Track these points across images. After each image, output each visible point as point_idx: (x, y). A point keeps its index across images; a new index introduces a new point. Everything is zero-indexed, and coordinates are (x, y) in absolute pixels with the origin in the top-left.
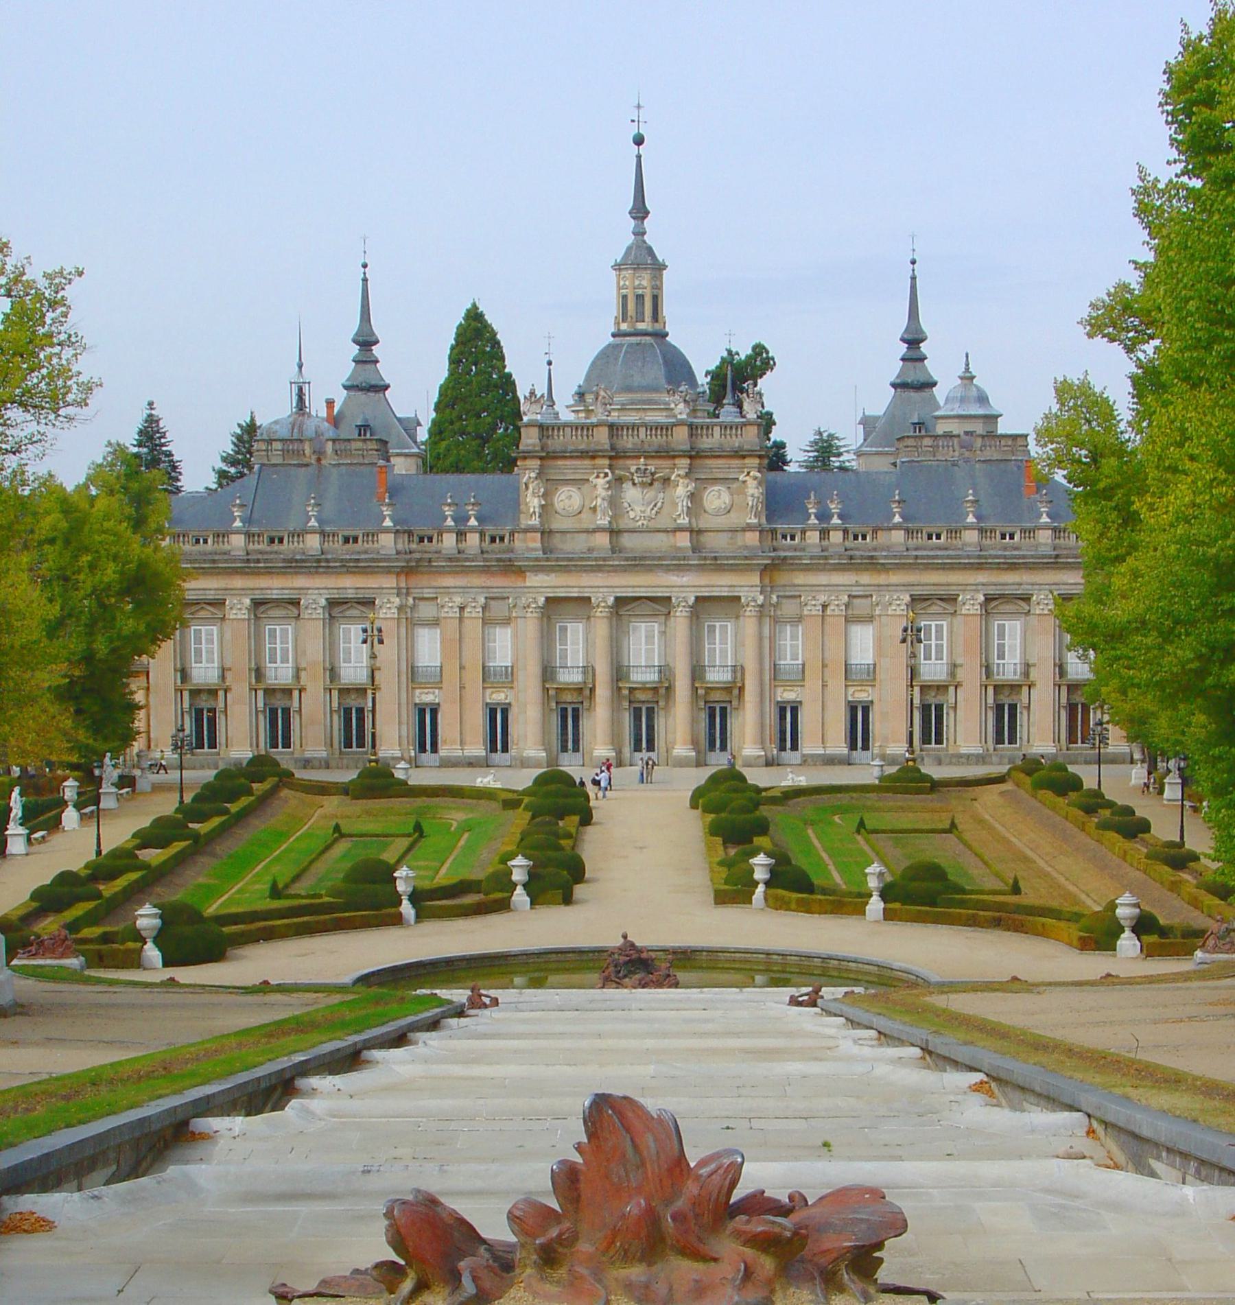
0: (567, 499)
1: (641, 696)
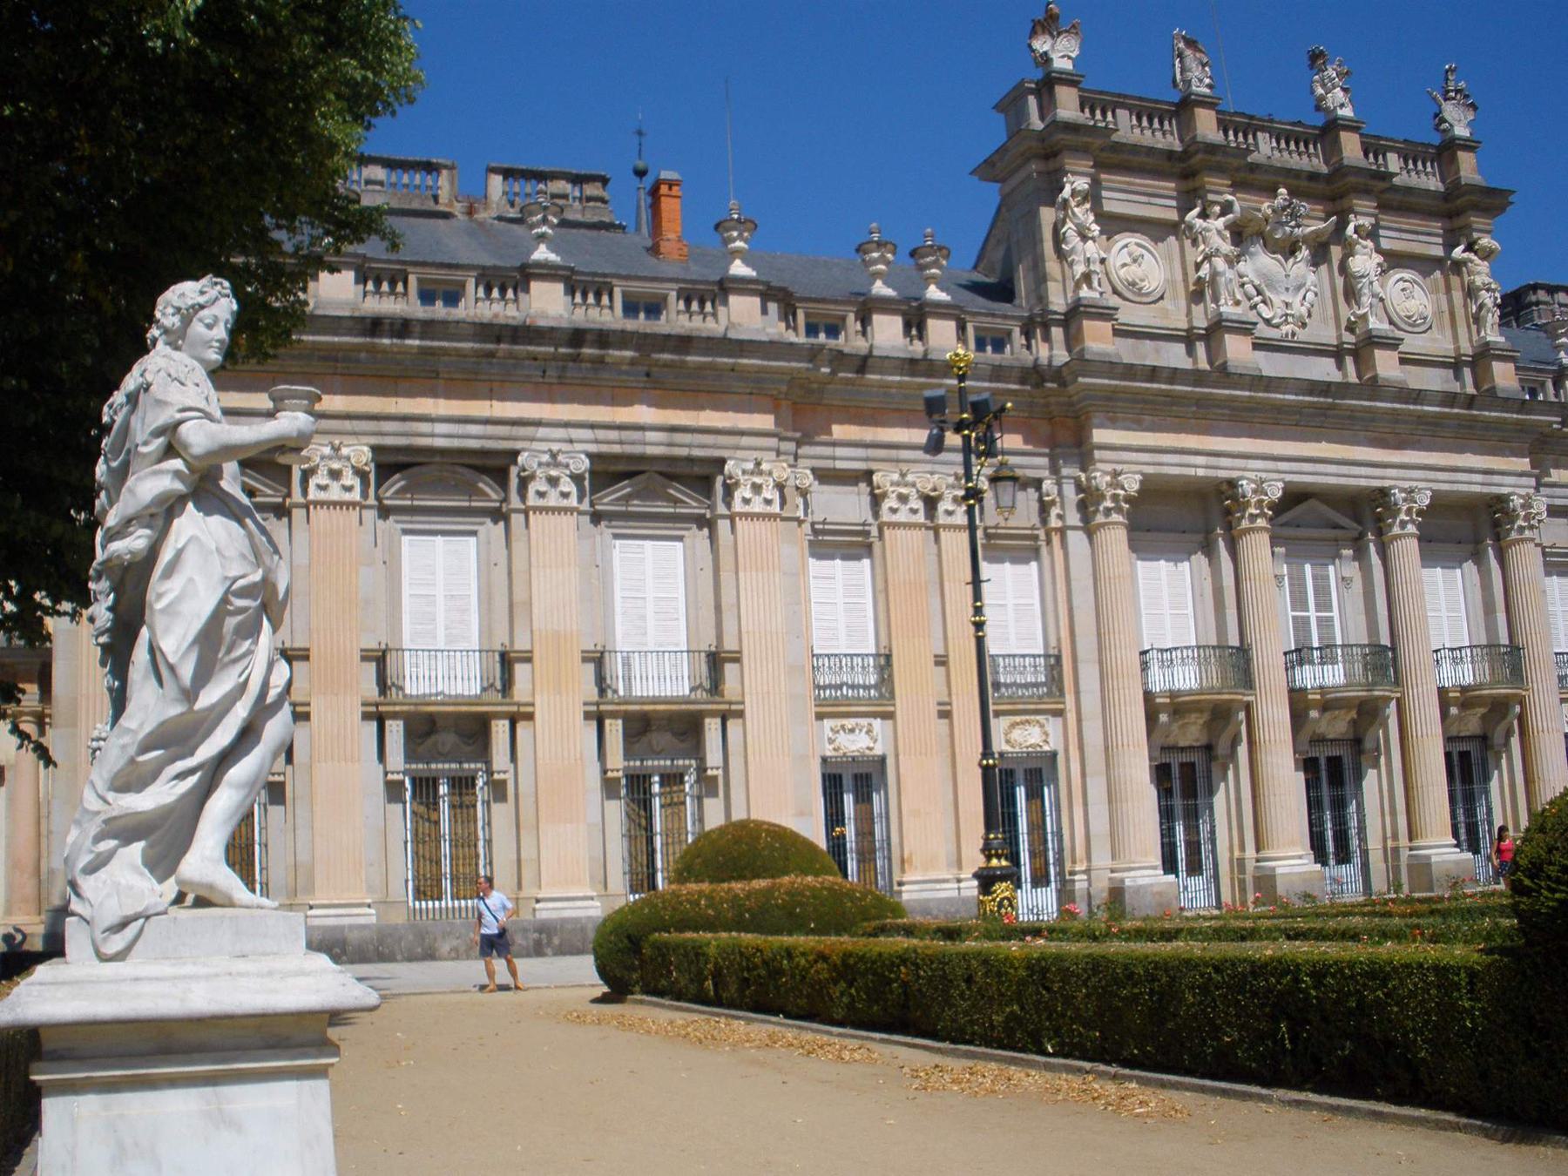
0: (1140, 265)
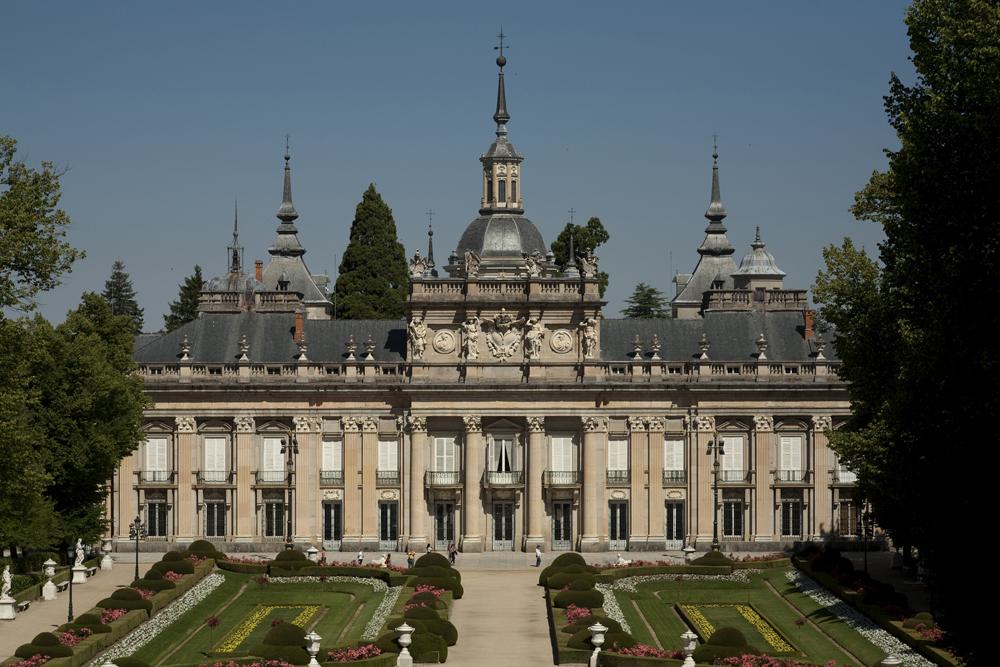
1: (500, 494)
